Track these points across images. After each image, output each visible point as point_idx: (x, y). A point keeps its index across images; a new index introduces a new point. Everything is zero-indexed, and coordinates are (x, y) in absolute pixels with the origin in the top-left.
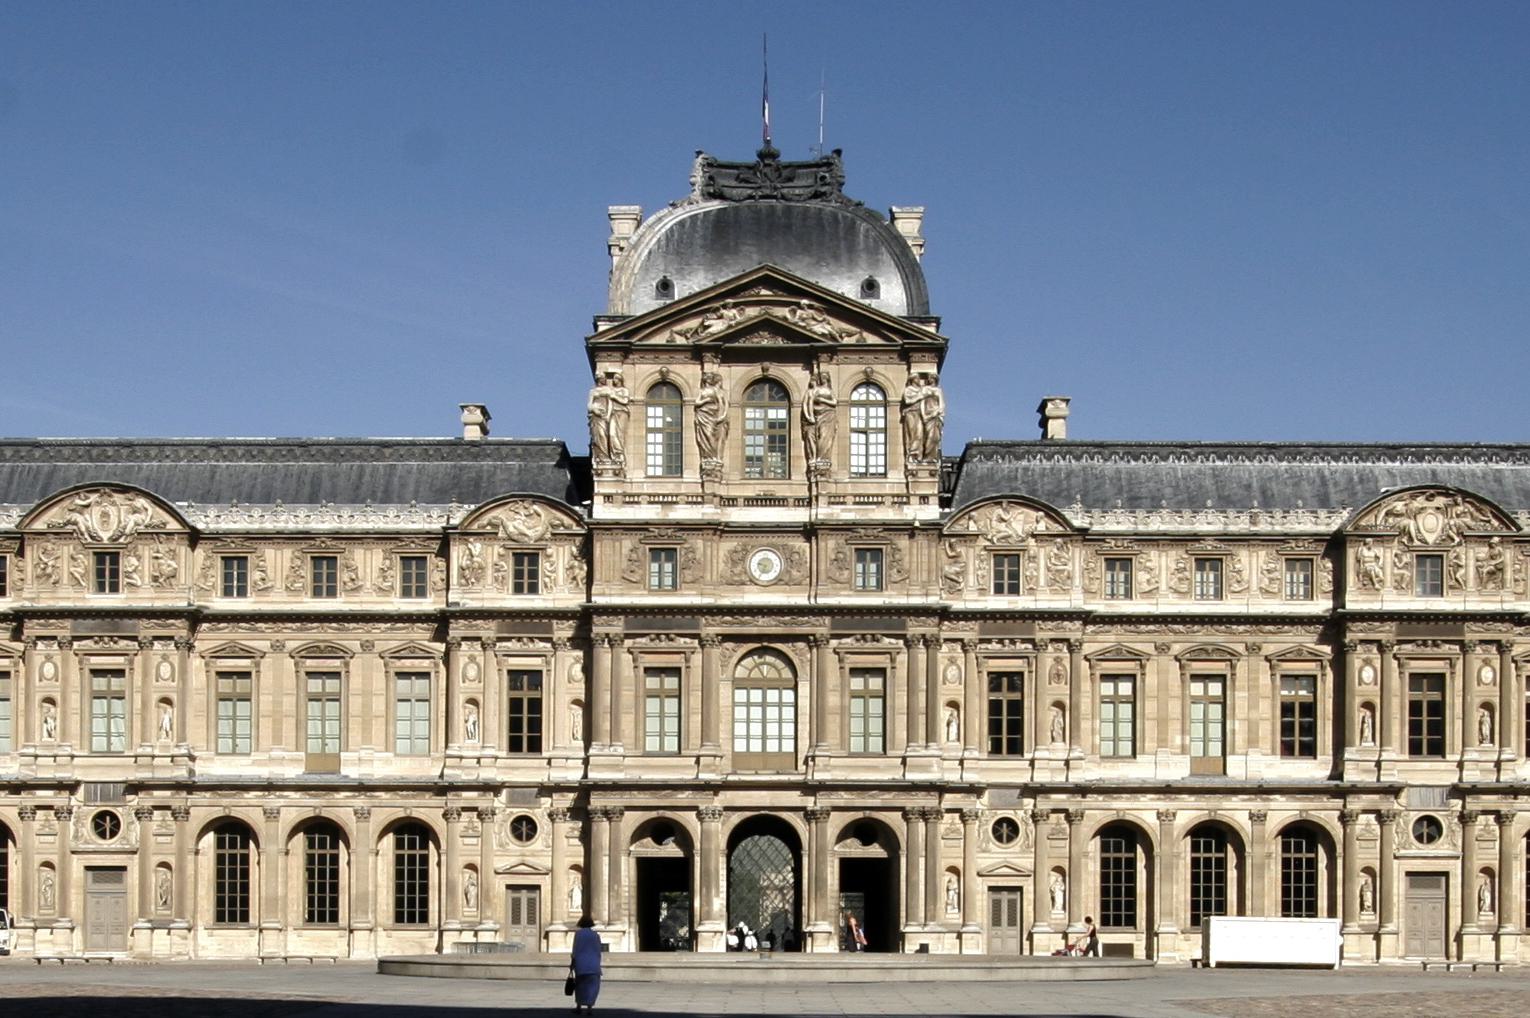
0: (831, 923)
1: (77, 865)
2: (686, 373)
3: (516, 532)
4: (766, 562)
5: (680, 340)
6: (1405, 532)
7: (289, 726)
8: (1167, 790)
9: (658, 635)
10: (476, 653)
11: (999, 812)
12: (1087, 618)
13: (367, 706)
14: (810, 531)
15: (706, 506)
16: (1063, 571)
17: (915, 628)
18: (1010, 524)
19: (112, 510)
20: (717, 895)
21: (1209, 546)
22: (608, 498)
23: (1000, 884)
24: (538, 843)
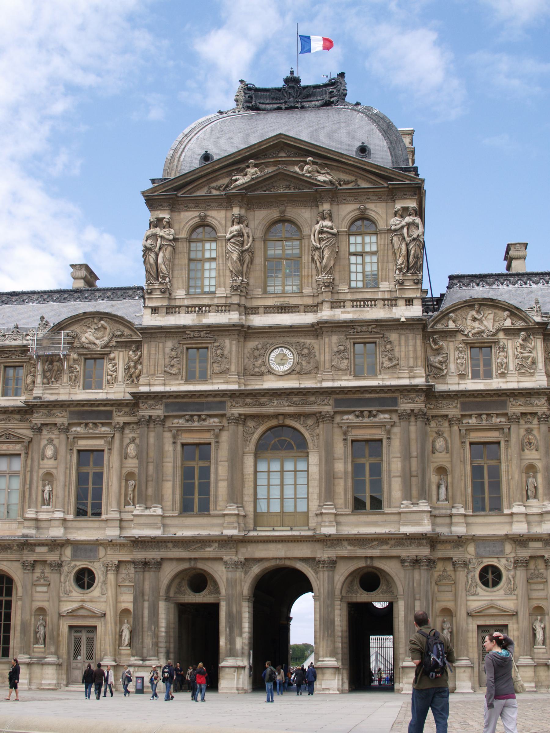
0: (337, 660)
2: (217, 216)
3: (87, 341)
5: (215, 192)
9: (192, 416)
10: (53, 437)
11: (485, 560)
14: (318, 330)
15: (232, 313)
16: (528, 357)
17: (405, 405)
18: (482, 322)
20: (241, 635)
23: (488, 623)
24: (96, 591)
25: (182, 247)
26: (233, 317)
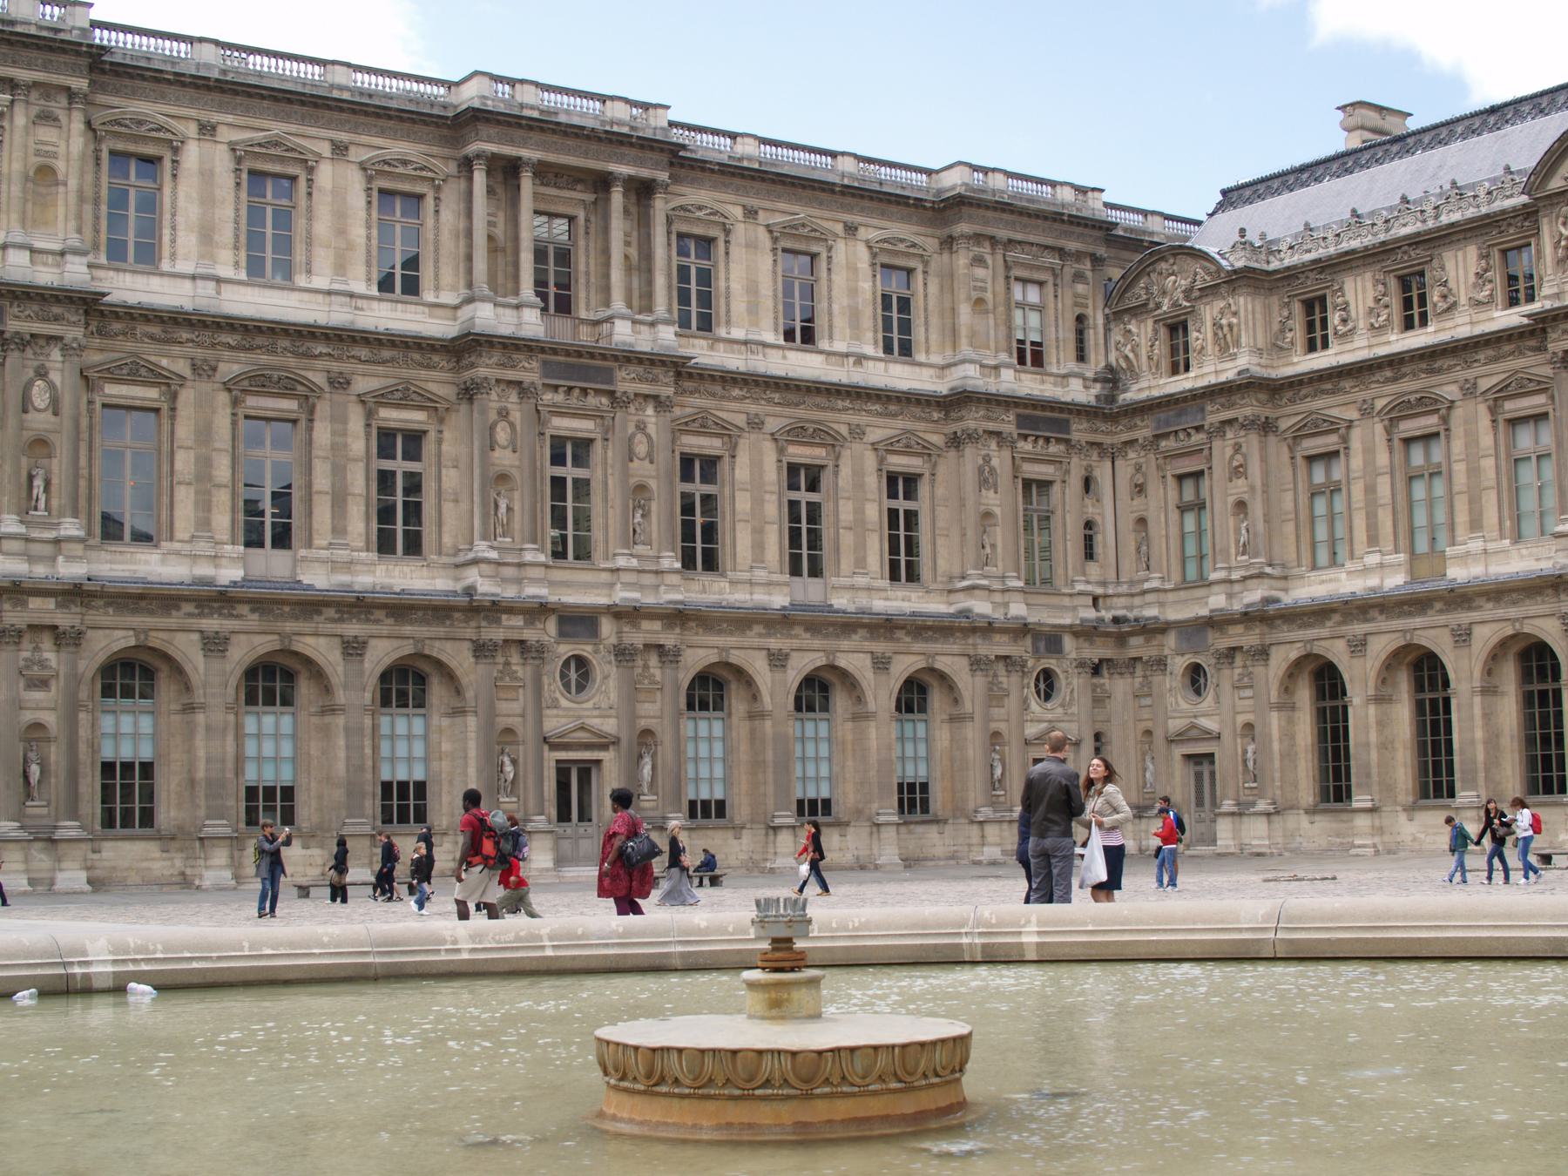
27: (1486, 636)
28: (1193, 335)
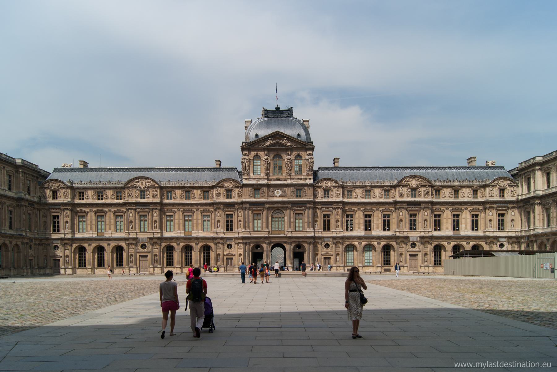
1: (138, 255)
2: (261, 153)
4: (278, 193)
6: (409, 185)
7: (181, 226)
8: (360, 238)
12: (344, 204)
13: (197, 222)
17: (308, 206)
19: (144, 182)
21: (368, 188)
22: (246, 179)
24: (232, 249)
25: (252, 161)
26: (266, 182)
27: (112, 245)
28: (58, 194)
